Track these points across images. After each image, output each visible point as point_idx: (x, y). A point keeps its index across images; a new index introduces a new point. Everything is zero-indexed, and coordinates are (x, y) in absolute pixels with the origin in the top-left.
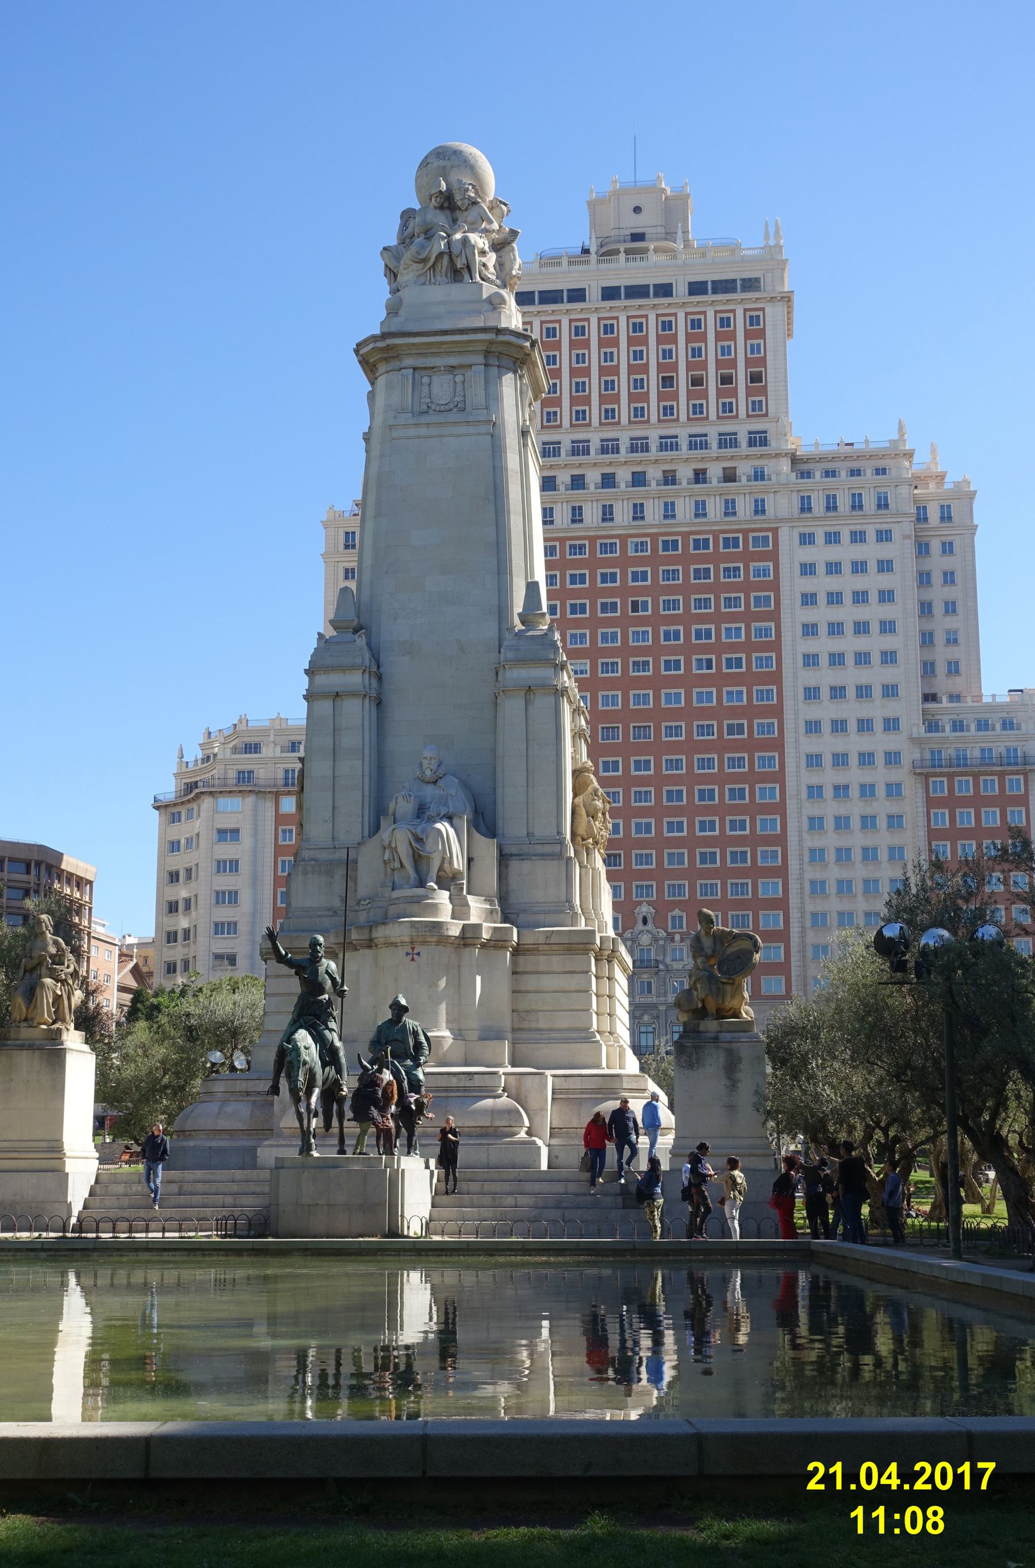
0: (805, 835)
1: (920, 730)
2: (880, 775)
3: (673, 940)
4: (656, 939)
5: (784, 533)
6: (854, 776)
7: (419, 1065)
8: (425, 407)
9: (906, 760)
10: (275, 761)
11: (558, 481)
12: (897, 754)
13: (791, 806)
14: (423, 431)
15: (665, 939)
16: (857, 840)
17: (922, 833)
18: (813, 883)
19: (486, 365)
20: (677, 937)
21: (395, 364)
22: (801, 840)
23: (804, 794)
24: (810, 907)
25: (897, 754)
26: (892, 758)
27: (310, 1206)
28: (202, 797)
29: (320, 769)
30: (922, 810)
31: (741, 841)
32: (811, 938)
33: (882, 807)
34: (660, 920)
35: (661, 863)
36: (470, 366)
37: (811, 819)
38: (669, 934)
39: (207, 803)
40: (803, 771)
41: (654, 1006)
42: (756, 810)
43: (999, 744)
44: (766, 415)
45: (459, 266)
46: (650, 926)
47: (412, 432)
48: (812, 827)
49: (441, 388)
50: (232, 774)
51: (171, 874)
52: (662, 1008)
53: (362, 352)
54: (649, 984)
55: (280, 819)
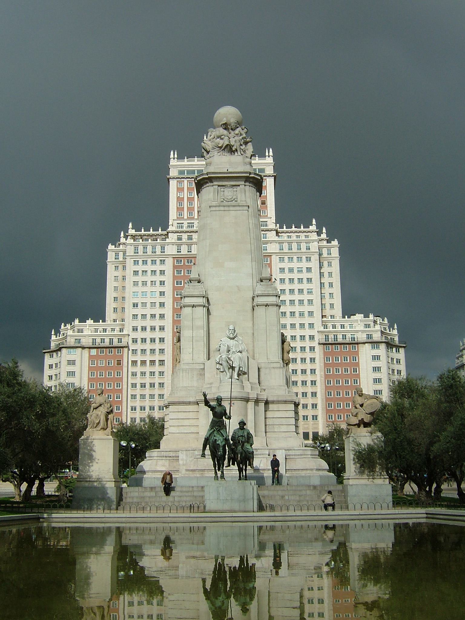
1: (322, 329)
5: (274, 257)
7: (251, 446)
8: (222, 200)
9: (316, 338)
10: (89, 336)
11: (193, 237)
14: (222, 208)
19: (245, 185)
21: (212, 184)
26: (312, 338)
27: (223, 500)
28: (62, 349)
29: (186, 334)
33: (308, 355)
36: (239, 186)
39: (64, 350)
44: (267, 216)
45: (234, 149)
47: (217, 208)
49: (228, 193)
50: (73, 340)
51: (49, 376)
53: (197, 179)
55: (90, 357)
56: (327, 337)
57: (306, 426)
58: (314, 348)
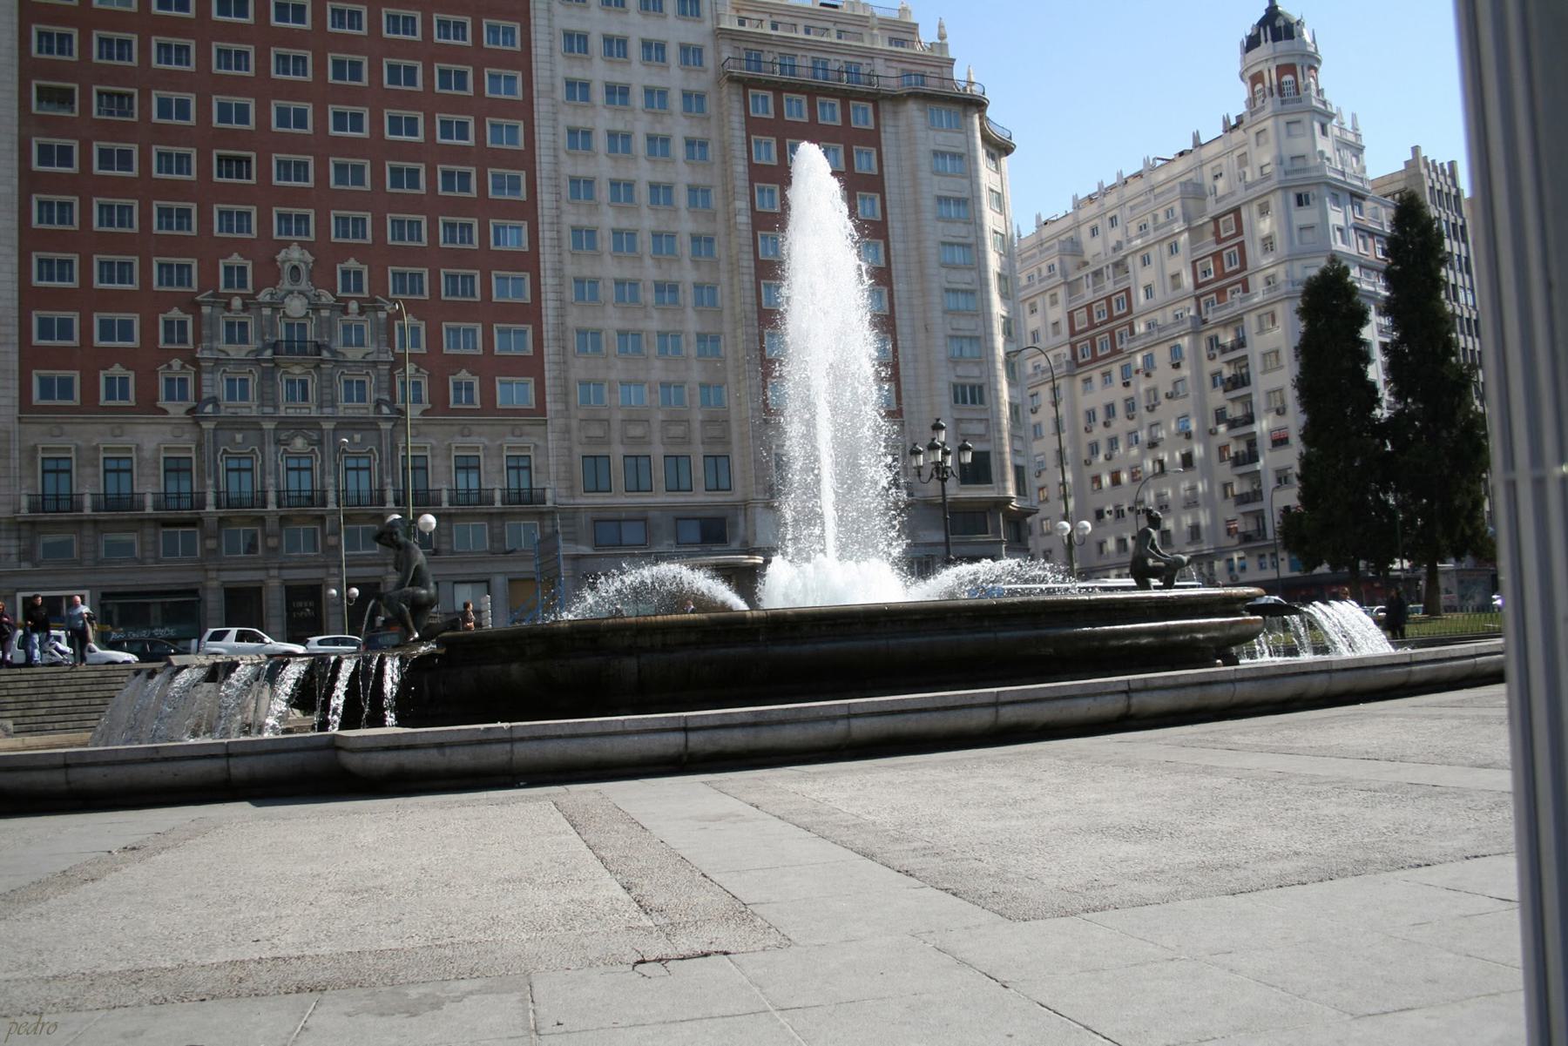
0: (563, 156)
2: (674, 78)
3: (345, 311)
4: (316, 308)
6: (637, 75)
9: (709, 61)
12: (698, 51)
13: (541, 107)
15: (332, 308)
16: (643, 172)
17: (740, 168)
18: (576, 230)
20: (353, 306)
22: (556, 163)
23: (561, 93)
24: (571, 270)
25: (698, 51)
26: (691, 54)
30: (739, 134)
31: (460, 155)
32: (574, 319)
34: (322, 273)
35: (322, 178)
37: (572, 132)
38: (339, 299)
40: (558, 57)
41: (313, 424)
42: (483, 108)
43: (838, 57)
46: (304, 284)
48: (573, 144)
52: (328, 426)
54: (304, 384)
56: (755, 60)
57: (677, 430)
58: (701, 97)
